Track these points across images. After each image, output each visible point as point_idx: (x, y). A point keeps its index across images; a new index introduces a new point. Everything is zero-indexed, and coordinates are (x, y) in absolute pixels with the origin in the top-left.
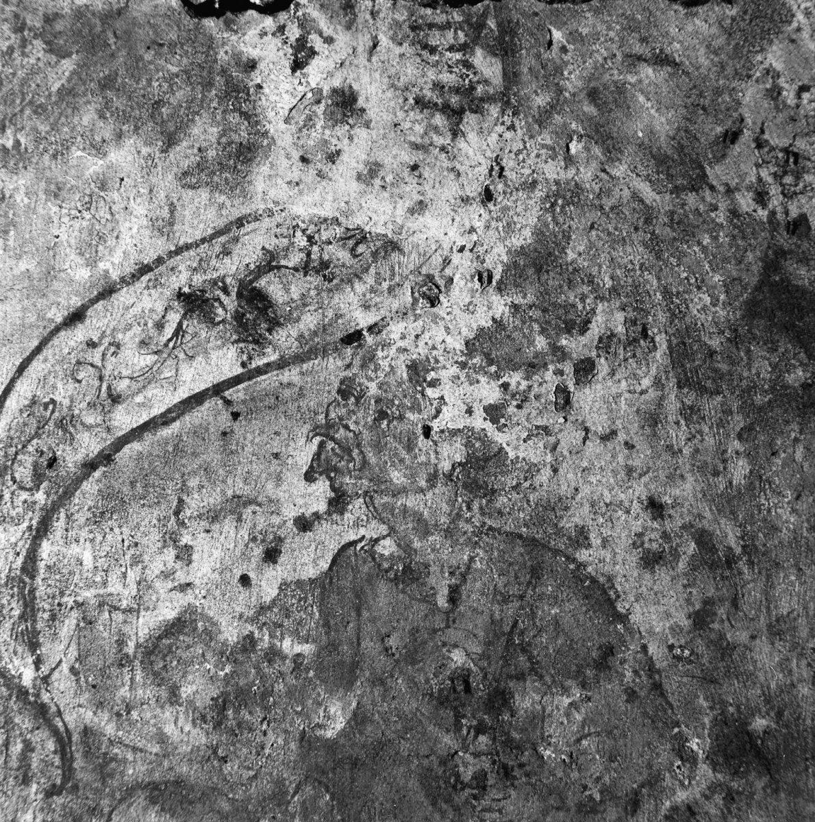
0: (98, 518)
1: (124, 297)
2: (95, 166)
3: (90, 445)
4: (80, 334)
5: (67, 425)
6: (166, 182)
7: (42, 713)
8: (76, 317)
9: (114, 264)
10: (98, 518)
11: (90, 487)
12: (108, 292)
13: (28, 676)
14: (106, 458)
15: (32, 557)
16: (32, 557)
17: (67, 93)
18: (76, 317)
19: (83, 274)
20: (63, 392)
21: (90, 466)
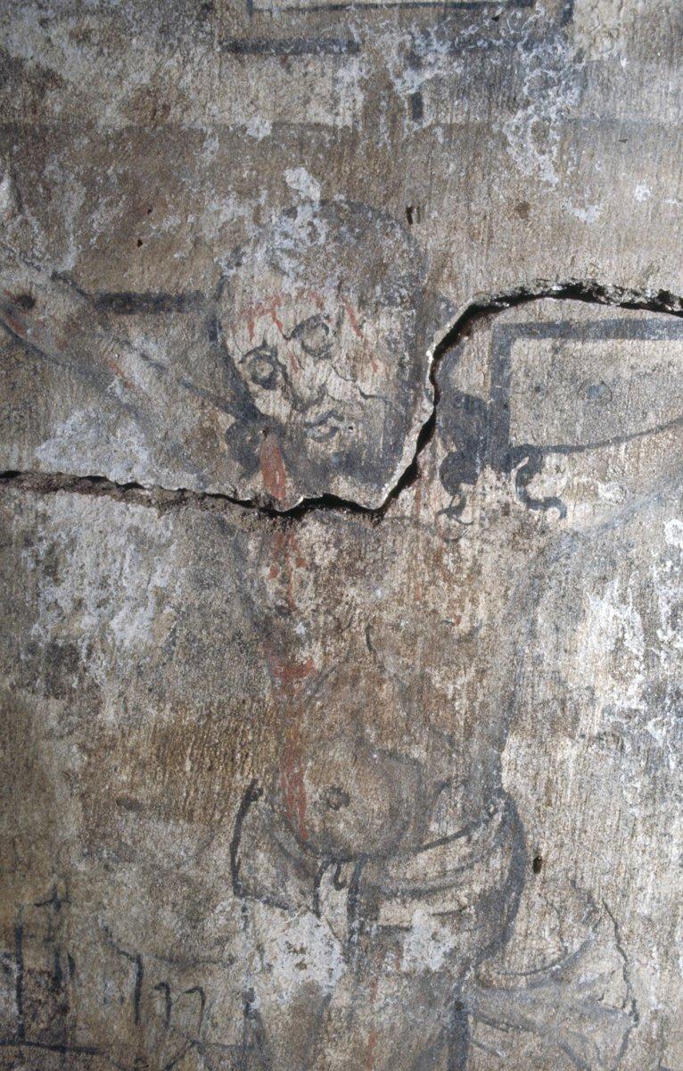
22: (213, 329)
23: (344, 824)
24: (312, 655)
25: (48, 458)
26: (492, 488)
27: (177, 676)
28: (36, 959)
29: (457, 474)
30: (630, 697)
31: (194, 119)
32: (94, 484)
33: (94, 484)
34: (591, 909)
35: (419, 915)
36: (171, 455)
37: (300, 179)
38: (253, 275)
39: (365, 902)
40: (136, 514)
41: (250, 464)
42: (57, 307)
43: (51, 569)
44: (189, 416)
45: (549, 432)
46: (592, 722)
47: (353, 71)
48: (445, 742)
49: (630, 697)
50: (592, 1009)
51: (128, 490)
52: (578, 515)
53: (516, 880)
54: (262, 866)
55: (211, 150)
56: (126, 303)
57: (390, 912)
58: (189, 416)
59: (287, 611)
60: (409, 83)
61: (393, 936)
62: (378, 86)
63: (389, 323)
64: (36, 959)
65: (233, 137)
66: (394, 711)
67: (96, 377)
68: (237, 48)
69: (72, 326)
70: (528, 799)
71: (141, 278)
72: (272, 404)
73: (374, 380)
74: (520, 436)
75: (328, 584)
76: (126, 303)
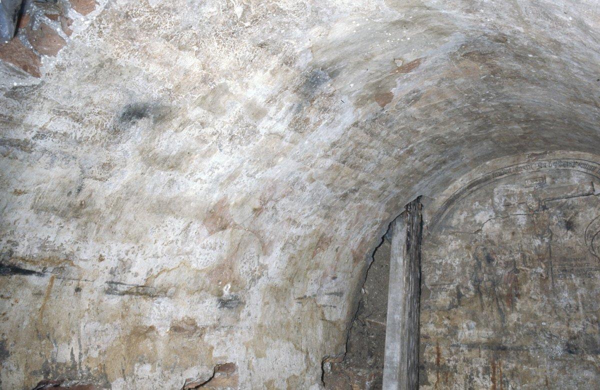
0: (597, 239)
1: (595, 221)
2: (589, 210)
3: (595, 233)
4: (591, 225)
5: (592, 232)
6: (596, 210)
7: (596, 256)
8: (591, 223)
9: (593, 218)
10: (597, 239)
11: (596, 237)
12: (593, 220)
13: (594, 253)
14: (597, 234)
15: (592, 243)
16: (592, 243)
17: (586, 205)
18: (591, 223)
19: (591, 219)
20: (591, 230)
21: (595, 235)
22: (526, 204)
23: (540, 233)
24: (536, 223)
25: (517, 213)
26: (546, 211)
27: (527, 225)
28: (520, 245)
29: (543, 210)
30: (557, 222)
31: (523, 192)
32: (520, 214)
33: (520, 214)
34: (557, 236)
35: (546, 239)
36: (525, 212)
37: (531, 195)
38: (528, 201)
39: (542, 238)
40: (523, 216)
41: (530, 211)
42: (517, 204)
43: (518, 220)
44: (526, 210)
45: (549, 207)
46: (555, 224)
47: (533, 188)
48: (546, 227)
49: (557, 222)
50: (559, 243)
51: (523, 214)
52: (552, 212)
53: (552, 235)
54: (535, 237)
55: (525, 194)
56: (520, 203)
57: (544, 238)
58: (526, 210)
59: (534, 220)
60: (536, 188)
61: (544, 240)
62: (535, 188)
63: (537, 202)
64: (520, 245)
65: (526, 192)
66: (542, 226)
67: (520, 208)
68: (526, 187)
69: (518, 205)
70: (552, 230)
71: (522, 202)
72: (531, 208)
73: (537, 205)
74: (547, 207)
75: (536, 218)
76: (520, 203)
